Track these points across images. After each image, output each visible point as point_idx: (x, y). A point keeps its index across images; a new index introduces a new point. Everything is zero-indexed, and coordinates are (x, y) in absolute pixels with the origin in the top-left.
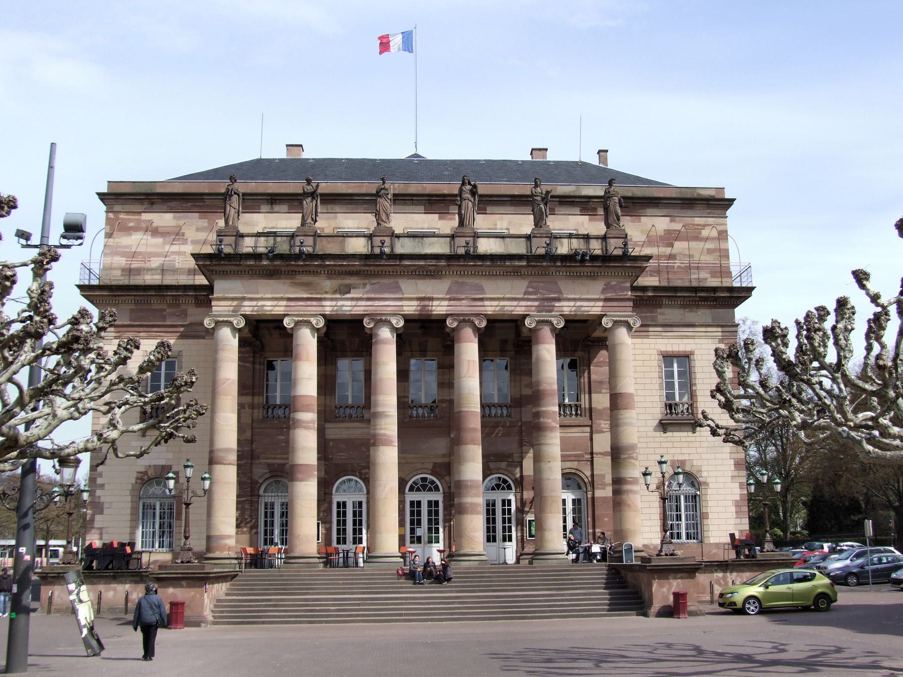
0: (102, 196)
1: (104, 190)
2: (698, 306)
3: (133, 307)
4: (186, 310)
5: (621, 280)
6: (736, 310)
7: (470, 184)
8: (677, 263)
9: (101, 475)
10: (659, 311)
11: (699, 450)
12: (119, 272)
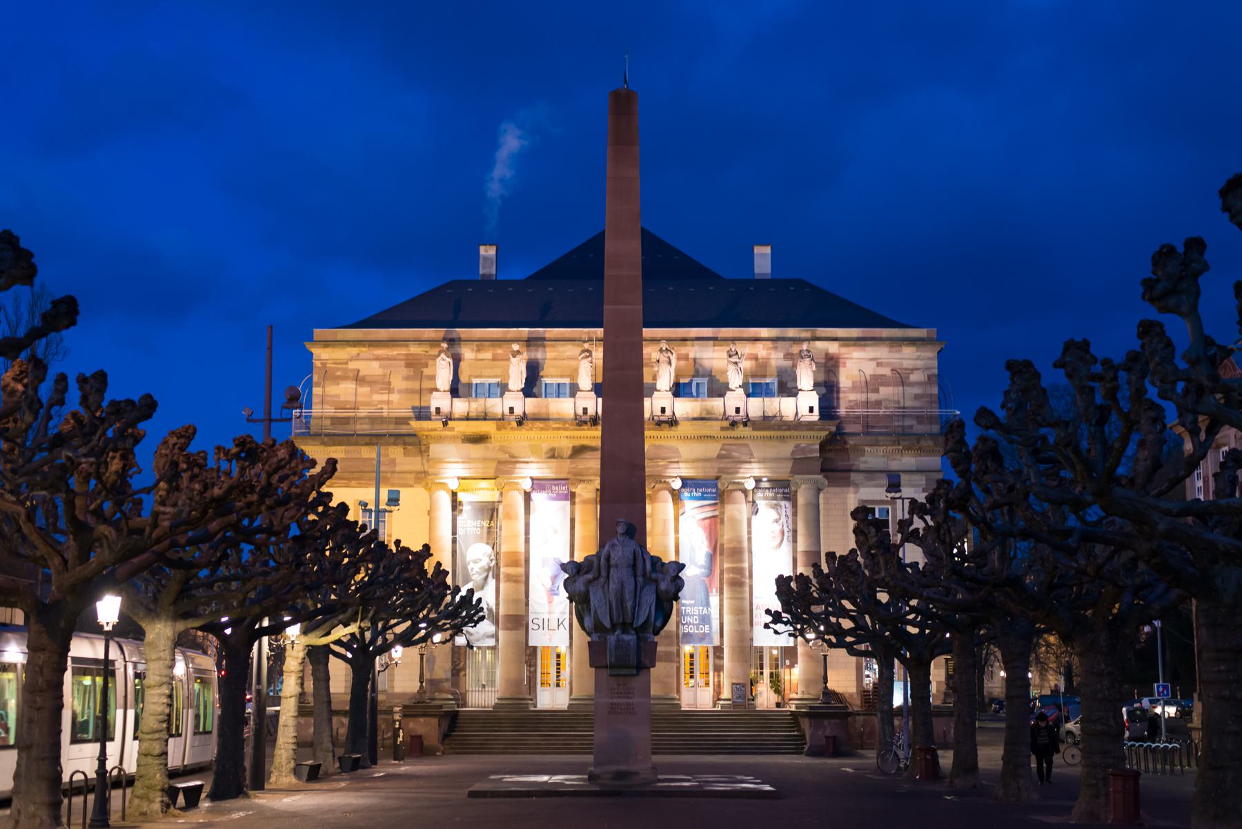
8: (882, 411)
10: (862, 459)
12: (328, 422)
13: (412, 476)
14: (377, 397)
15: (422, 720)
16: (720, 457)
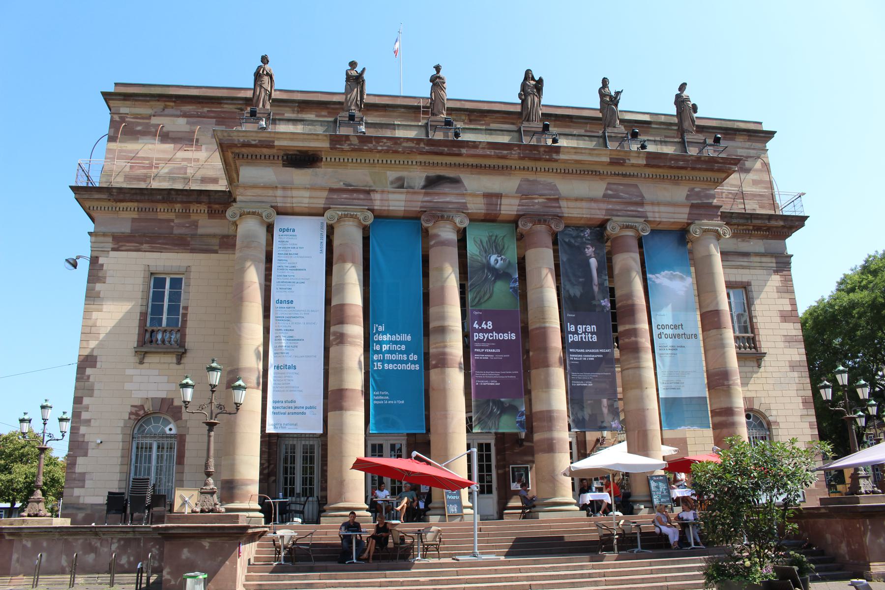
0: (107, 96)
1: (111, 89)
2: (751, 236)
3: (136, 216)
4: (197, 222)
5: (705, 187)
6: (788, 241)
7: (533, 79)
9: (87, 408)
11: (766, 387)
13: (216, 241)
14: (181, 155)
15: (206, 543)
16: (605, 196)
